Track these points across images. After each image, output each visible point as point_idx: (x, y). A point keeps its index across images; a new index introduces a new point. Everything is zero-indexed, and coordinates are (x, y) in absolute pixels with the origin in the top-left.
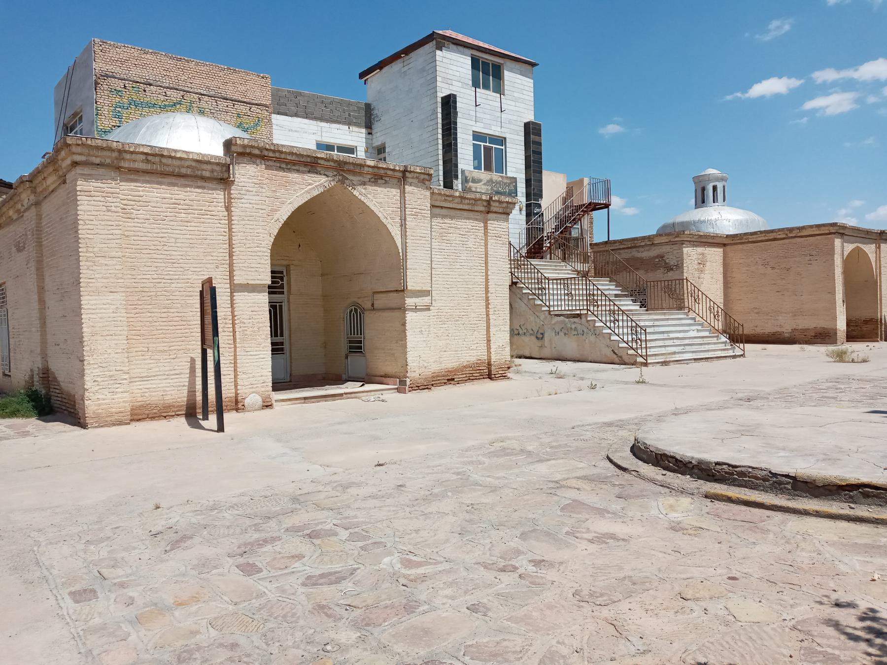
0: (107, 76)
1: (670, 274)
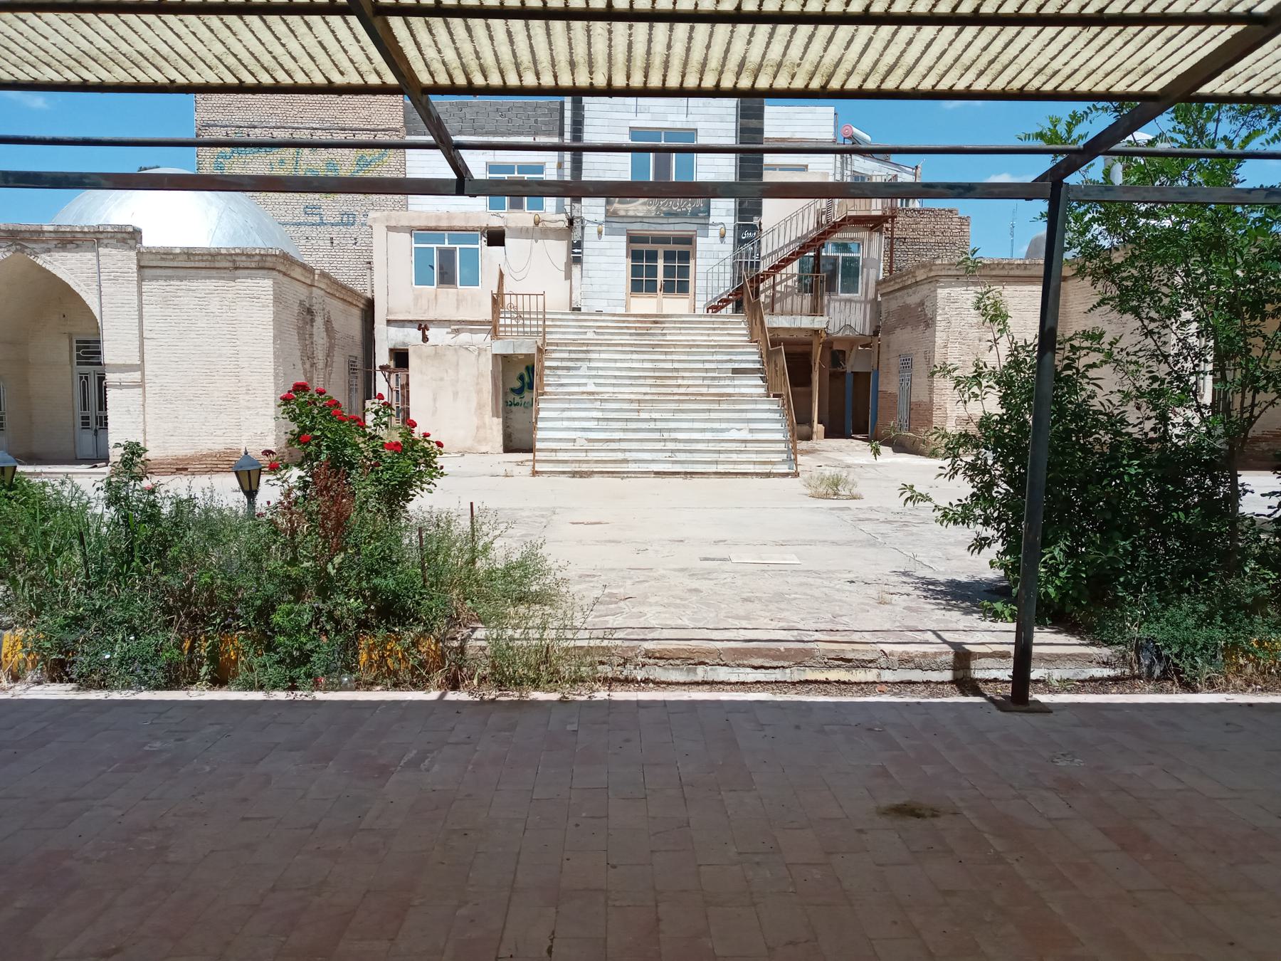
0: (209, 126)
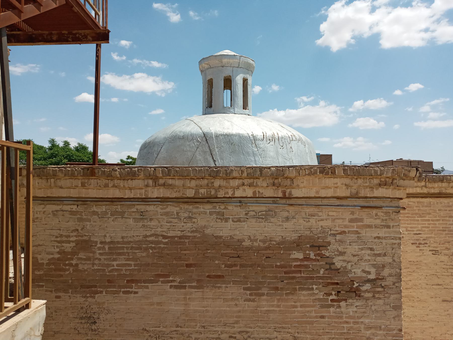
1: (350, 308)
